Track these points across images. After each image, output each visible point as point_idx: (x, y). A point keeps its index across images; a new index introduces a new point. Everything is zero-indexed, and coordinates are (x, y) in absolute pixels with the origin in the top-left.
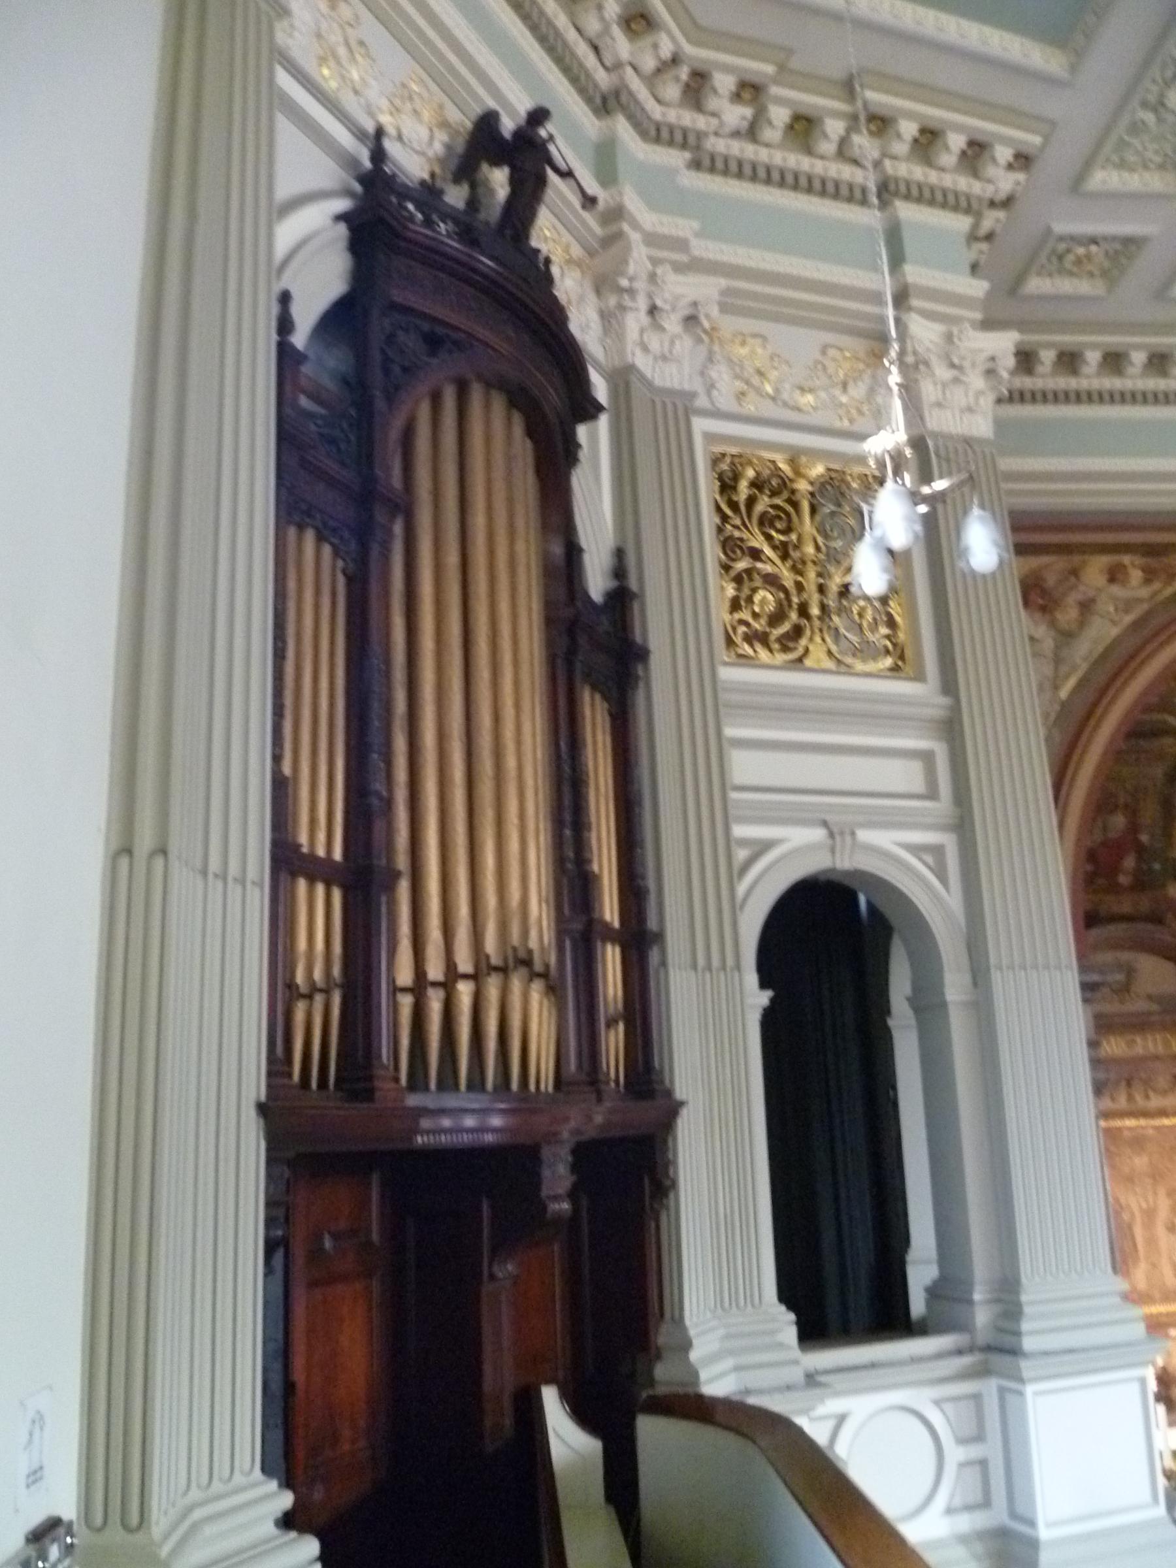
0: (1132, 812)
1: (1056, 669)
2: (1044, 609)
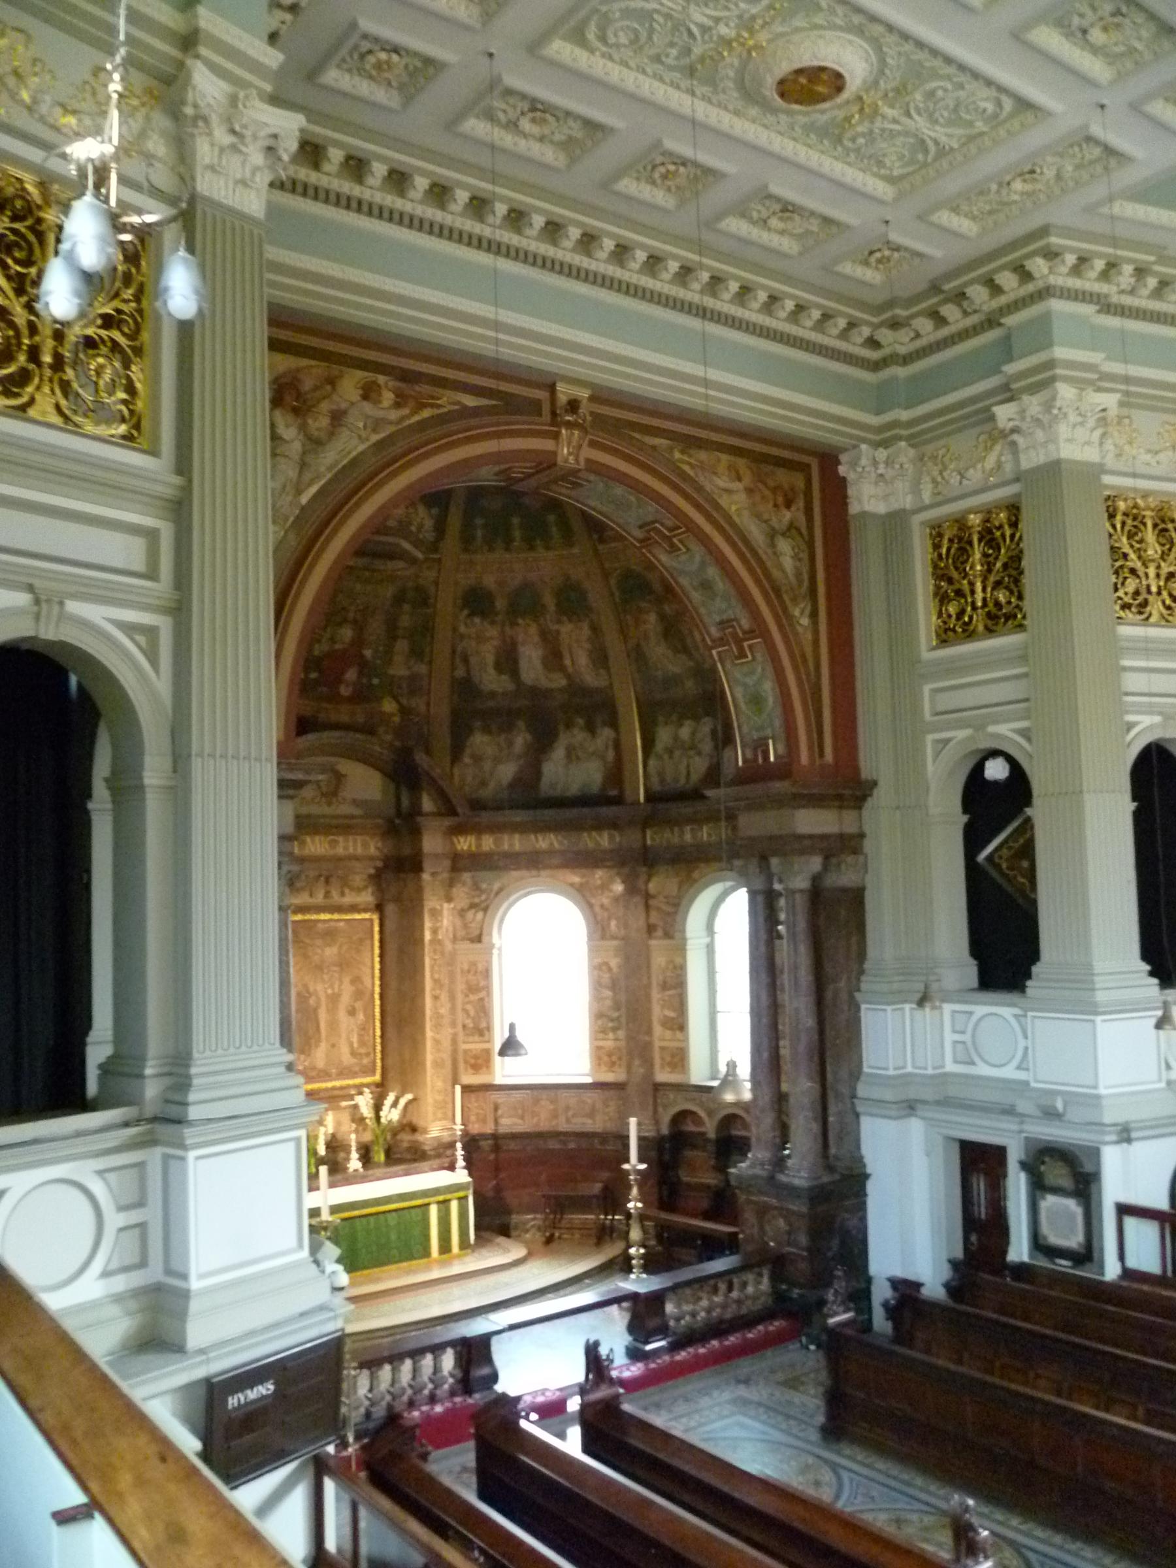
0: (360, 627)
1: (301, 473)
2: (296, 411)
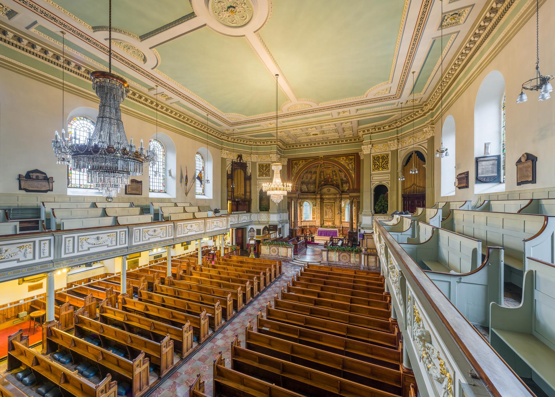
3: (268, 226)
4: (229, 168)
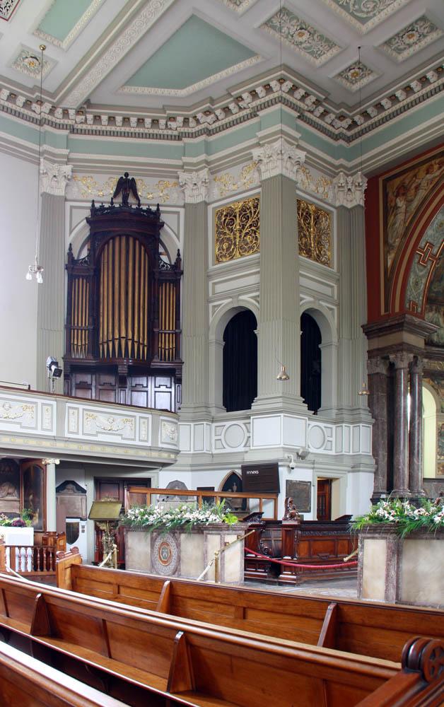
2: (403, 194)
3: (239, 472)
4: (76, 233)
